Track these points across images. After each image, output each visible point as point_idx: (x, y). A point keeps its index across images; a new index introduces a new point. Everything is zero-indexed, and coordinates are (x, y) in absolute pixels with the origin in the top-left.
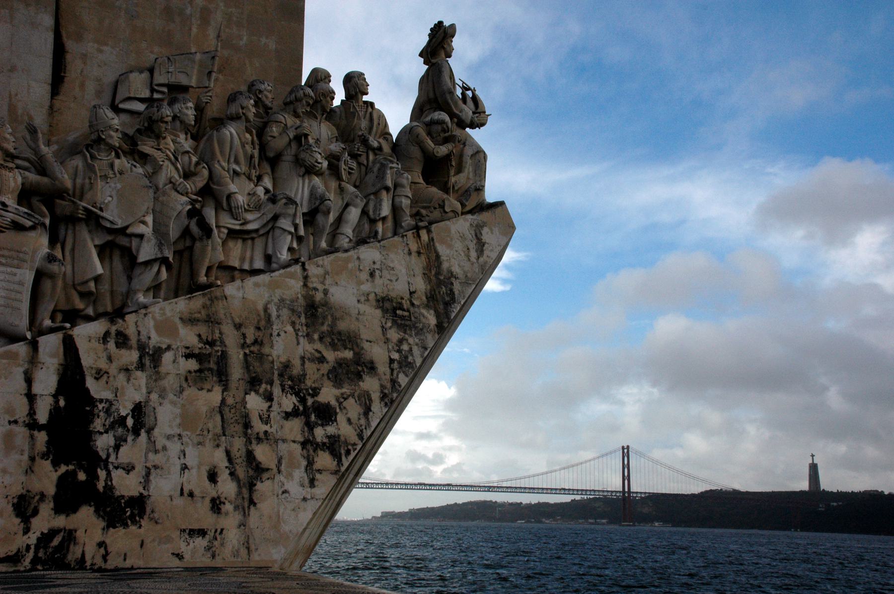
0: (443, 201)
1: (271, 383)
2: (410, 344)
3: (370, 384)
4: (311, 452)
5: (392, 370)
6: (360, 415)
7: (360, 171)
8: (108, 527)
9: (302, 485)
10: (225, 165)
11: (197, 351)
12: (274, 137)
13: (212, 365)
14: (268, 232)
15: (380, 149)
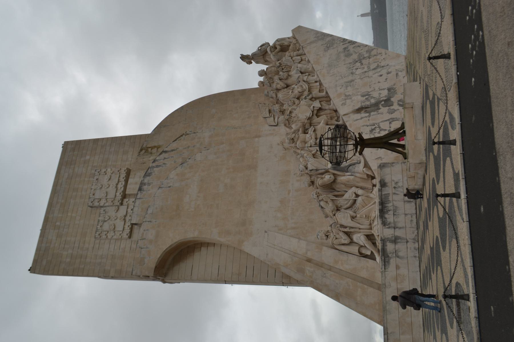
0: (294, 44)
1: (353, 69)
2: (337, 42)
3: (351, 48)
4: (372, 56)
5: (346, 44)
6: (360, 48)
7: (287, 68)
8: (396, 93)
9: (382, 55)
10: (290, 95)
11: (345, 88)
12: (281, 85)
13: (349, 84)
14: (308, 83)
15: (280, 63)
